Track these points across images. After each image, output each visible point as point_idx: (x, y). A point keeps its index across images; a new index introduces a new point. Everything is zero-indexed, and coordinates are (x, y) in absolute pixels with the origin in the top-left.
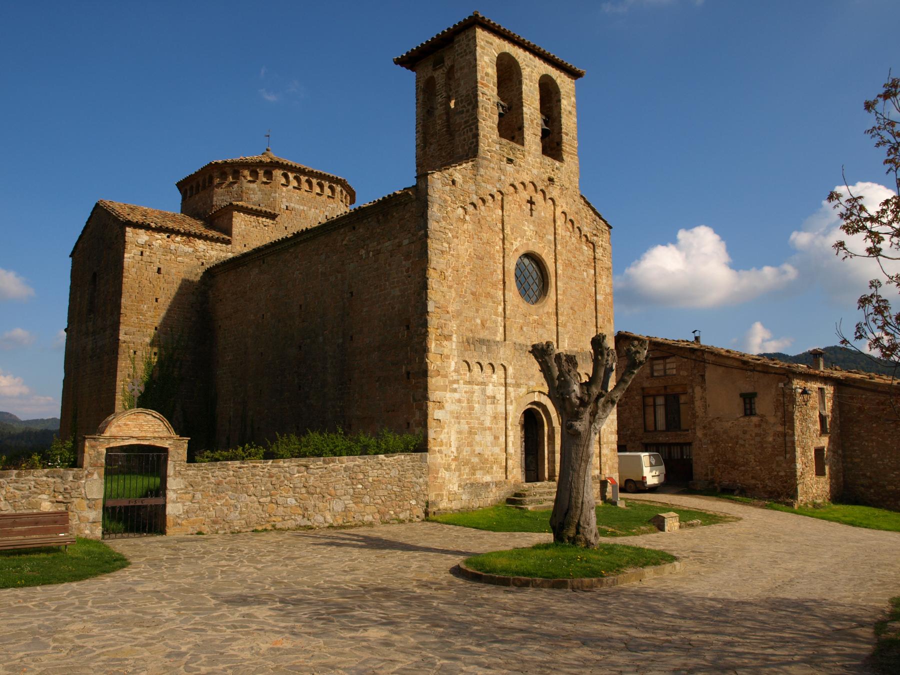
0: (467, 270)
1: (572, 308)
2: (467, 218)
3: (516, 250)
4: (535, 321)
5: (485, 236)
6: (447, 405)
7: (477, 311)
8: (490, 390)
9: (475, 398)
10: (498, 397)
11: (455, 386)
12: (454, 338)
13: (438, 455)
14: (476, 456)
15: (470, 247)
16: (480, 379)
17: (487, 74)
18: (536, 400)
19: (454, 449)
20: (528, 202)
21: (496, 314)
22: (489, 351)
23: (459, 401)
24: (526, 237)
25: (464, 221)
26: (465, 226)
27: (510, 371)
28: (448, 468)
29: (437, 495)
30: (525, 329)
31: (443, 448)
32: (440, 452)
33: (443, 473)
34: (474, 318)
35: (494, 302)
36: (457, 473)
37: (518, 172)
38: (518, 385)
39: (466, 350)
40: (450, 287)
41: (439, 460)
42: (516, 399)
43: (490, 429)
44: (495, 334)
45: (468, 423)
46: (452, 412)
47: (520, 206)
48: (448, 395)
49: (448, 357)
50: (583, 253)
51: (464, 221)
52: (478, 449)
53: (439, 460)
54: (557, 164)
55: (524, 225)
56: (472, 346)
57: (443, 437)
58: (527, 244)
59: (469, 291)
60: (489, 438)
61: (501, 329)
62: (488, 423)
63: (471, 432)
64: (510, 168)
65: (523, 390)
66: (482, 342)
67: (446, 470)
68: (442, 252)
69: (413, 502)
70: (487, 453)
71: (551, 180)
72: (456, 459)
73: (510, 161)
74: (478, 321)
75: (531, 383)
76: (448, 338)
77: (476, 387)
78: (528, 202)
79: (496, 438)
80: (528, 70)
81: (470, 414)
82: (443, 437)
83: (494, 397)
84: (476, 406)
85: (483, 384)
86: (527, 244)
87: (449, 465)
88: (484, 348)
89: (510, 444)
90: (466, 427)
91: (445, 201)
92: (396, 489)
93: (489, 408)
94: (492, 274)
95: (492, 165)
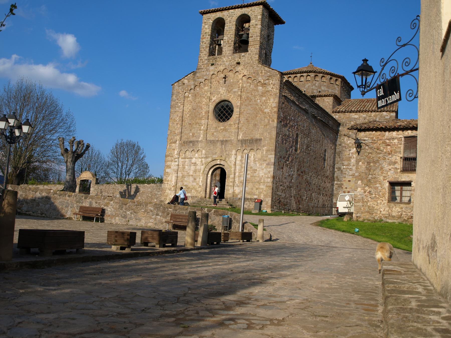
0: (188, 115)
1: (246, 119)
2: (190, 95)
3: (214, 101)
4: (221, 129)
5: (197, 100)
6: (172, 167)
7: (191, 130)
8: (194, 160)
9: (186, 164)
10: (197, 163)
11: (176, 160)
12: (178, 142)
13: (166, 184)
14: (185, 186)
15: (190, 106)
16: (189, 157)
17: (206, 33)
18: (218, 163)
19: (173, 183)
20: (224, 78)
21: (200, 130)
22: (193, 145)
23: (178, 165)
24: (222, 93)
25: (188, 97)
26: (189, 99)
27: (204, 152)
28: (170, 189)
29: (164, 199)
30: (215, 134)
31: (169, 182)
32: (167, 183)
33: (168, 191)
34: (189, 133)
35: (199, 125)
36: (174, 192)
37: (216, 68)
38: (206, 158)
39: (182, 145)
40: (177, 124)
41: (167, 186)
42: (205, 163)
43: (192, 176)
44: (199, 138)
45: (182, 173)
46: (174, 169)
47: (218, 82)
48: (173, 163)
49: (174, 150)
50: (258, 91)
51: (188, 97)
52: (185, 183)
53: (167, 186)
54: (243, 54)
55: (219, 89)
56: (185, 144)
57: (169, 178)
58: (221, 97)
59: (187, 123)
60: (191, 179)
61: (202, 136)
62: (191, 173)
63: (182, 177)
64: (212, 68)
65: (210, 159)
66: (191, 142)
67: (169, 190)
68: (176, 112)
69: (155, 200)
70: (190, 185)
71: (238, 63)
72: (173, 186)
73: (212, 65)
74: (191, 134)
75: (214, 156)
76: (175, 142)
77: (187, 160)
78: (224, 78)
79: (195, 179)
80: (229, 19)
81: (183, 170)
82: (169, 178)
83: (196, 163)
84: (186, 167)
85: (191, 158)
86: (221, 97)
87: (171, 188)
88: (191, 144)
89: (200, 182)
90: (181, 175)
91: (179, 93)
92: (150, 195)
93: (193, 168)
94: (200, 114)
95: (203, 70)
